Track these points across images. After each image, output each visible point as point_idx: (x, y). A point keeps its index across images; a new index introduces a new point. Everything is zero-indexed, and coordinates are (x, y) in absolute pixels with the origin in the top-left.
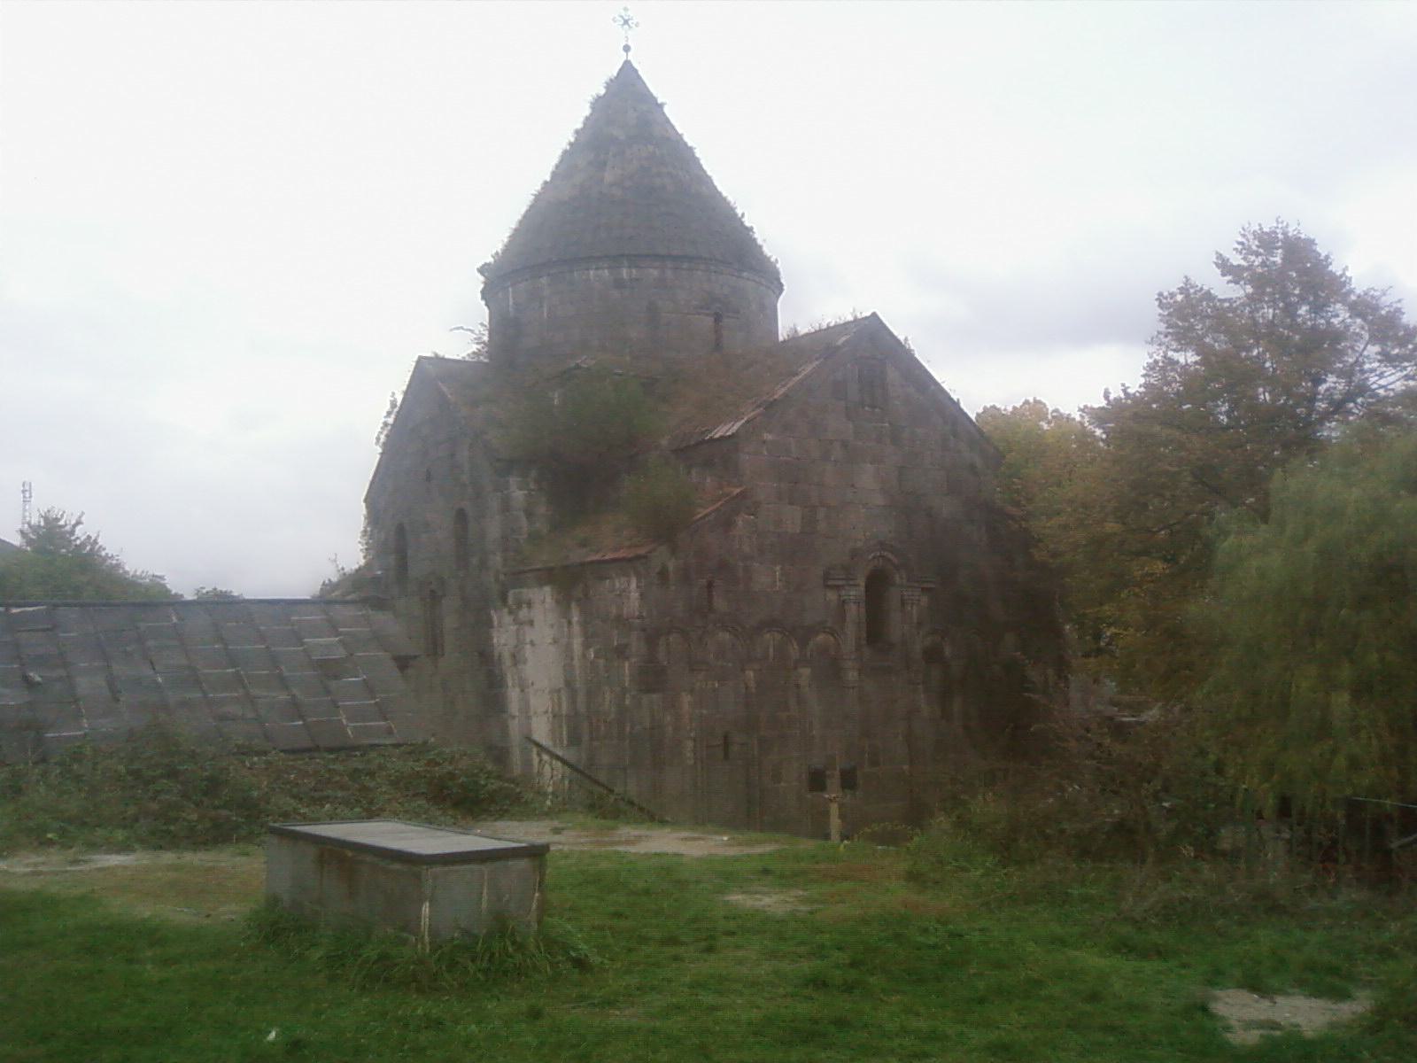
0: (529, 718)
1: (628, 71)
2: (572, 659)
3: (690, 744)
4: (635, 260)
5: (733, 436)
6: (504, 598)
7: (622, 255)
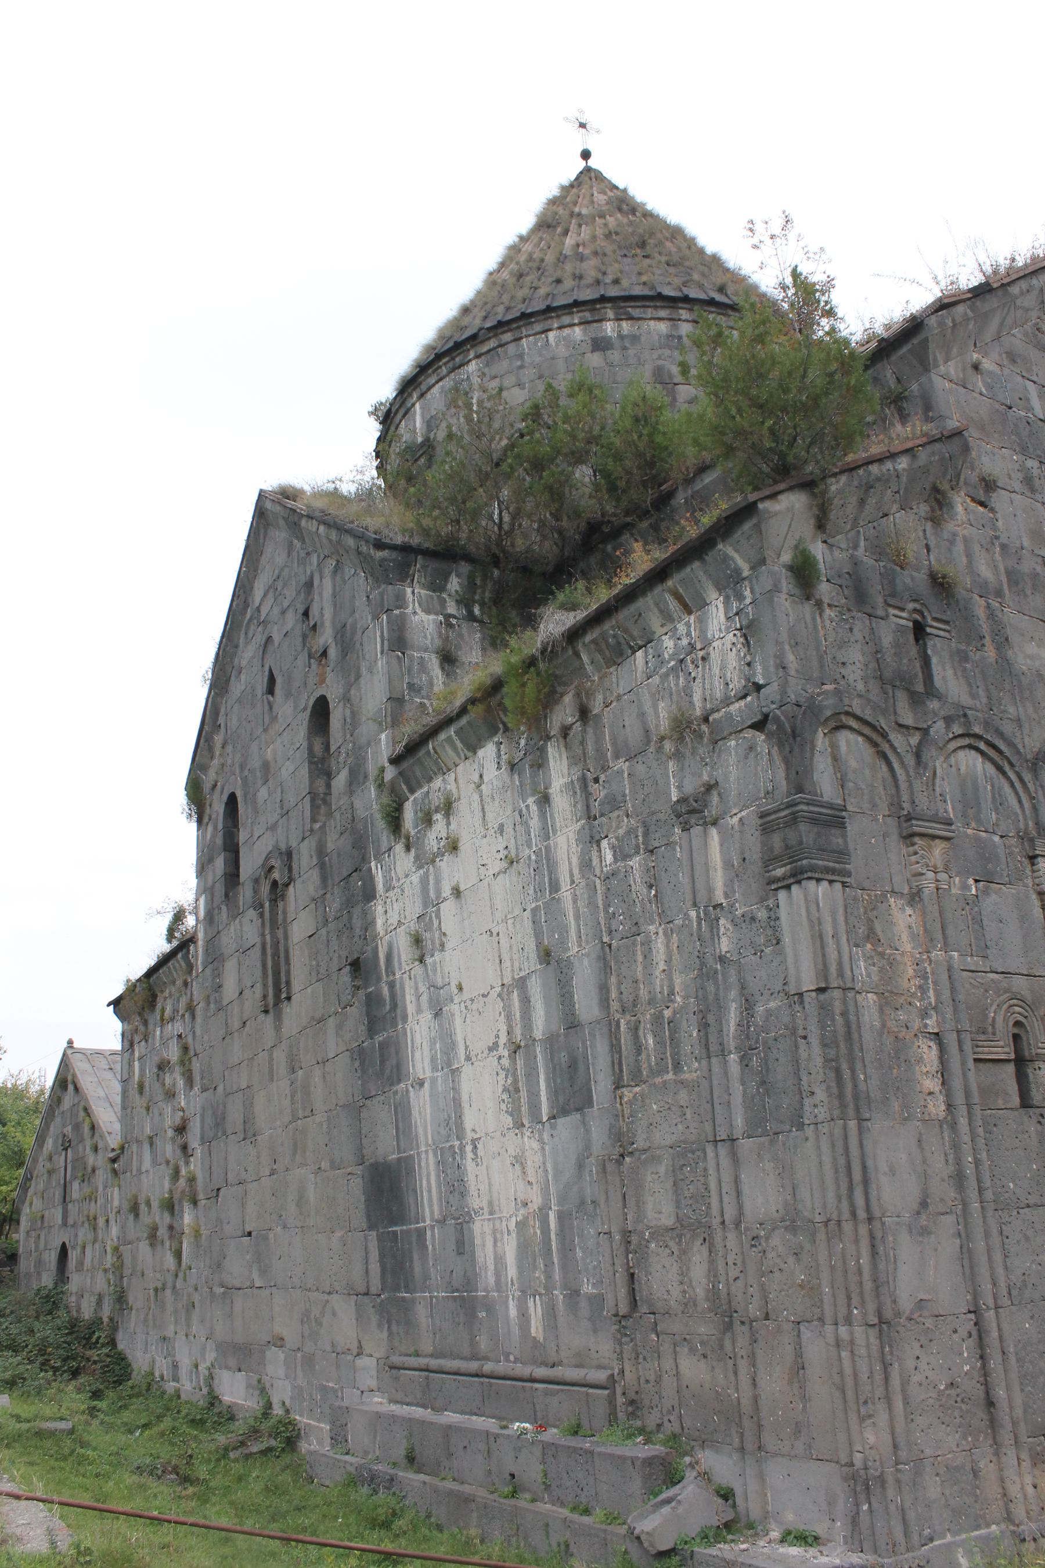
0: (455, 1072)
2: (555, 887)
3: (929, 1053)
4: (624, 304)
6: (395, 822)
7: (603, 299)
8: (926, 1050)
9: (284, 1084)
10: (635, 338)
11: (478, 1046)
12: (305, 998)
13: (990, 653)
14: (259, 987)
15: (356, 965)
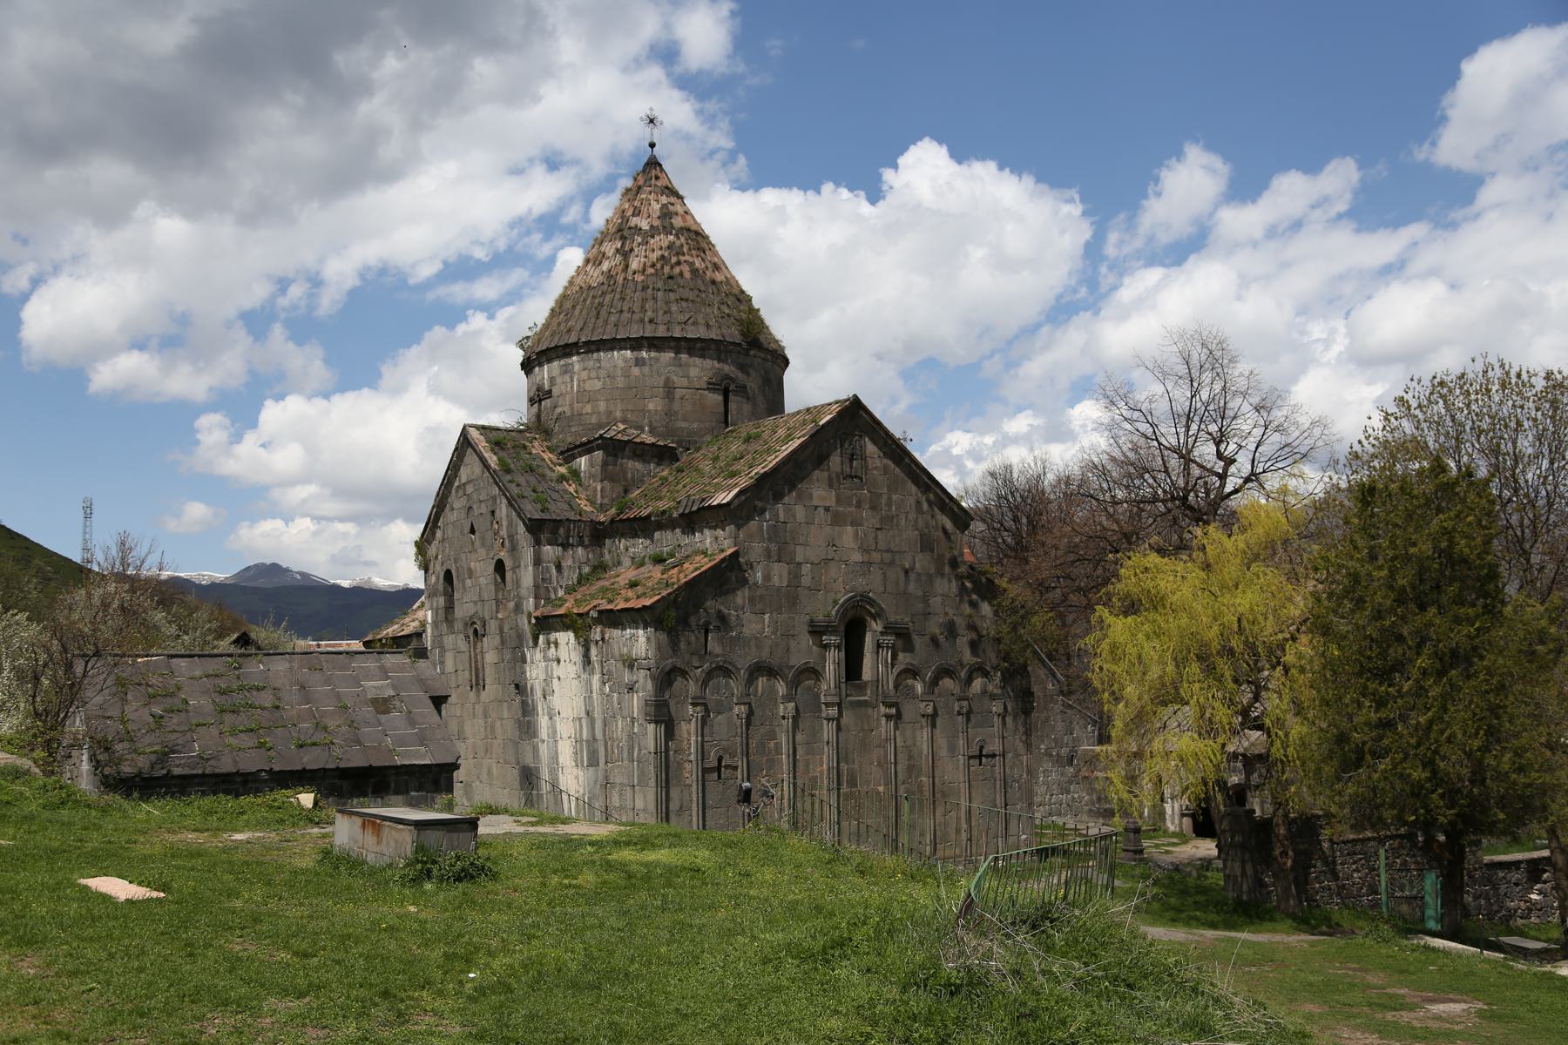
1: (653, 164)
4: (655, 343)
5: (728, 504)
6: (536, 639)
9: (481, 722)
10: (657, 359)
11: (565, 736)
12: (492, 690)
14: (467, 673)
15: (517, 686)
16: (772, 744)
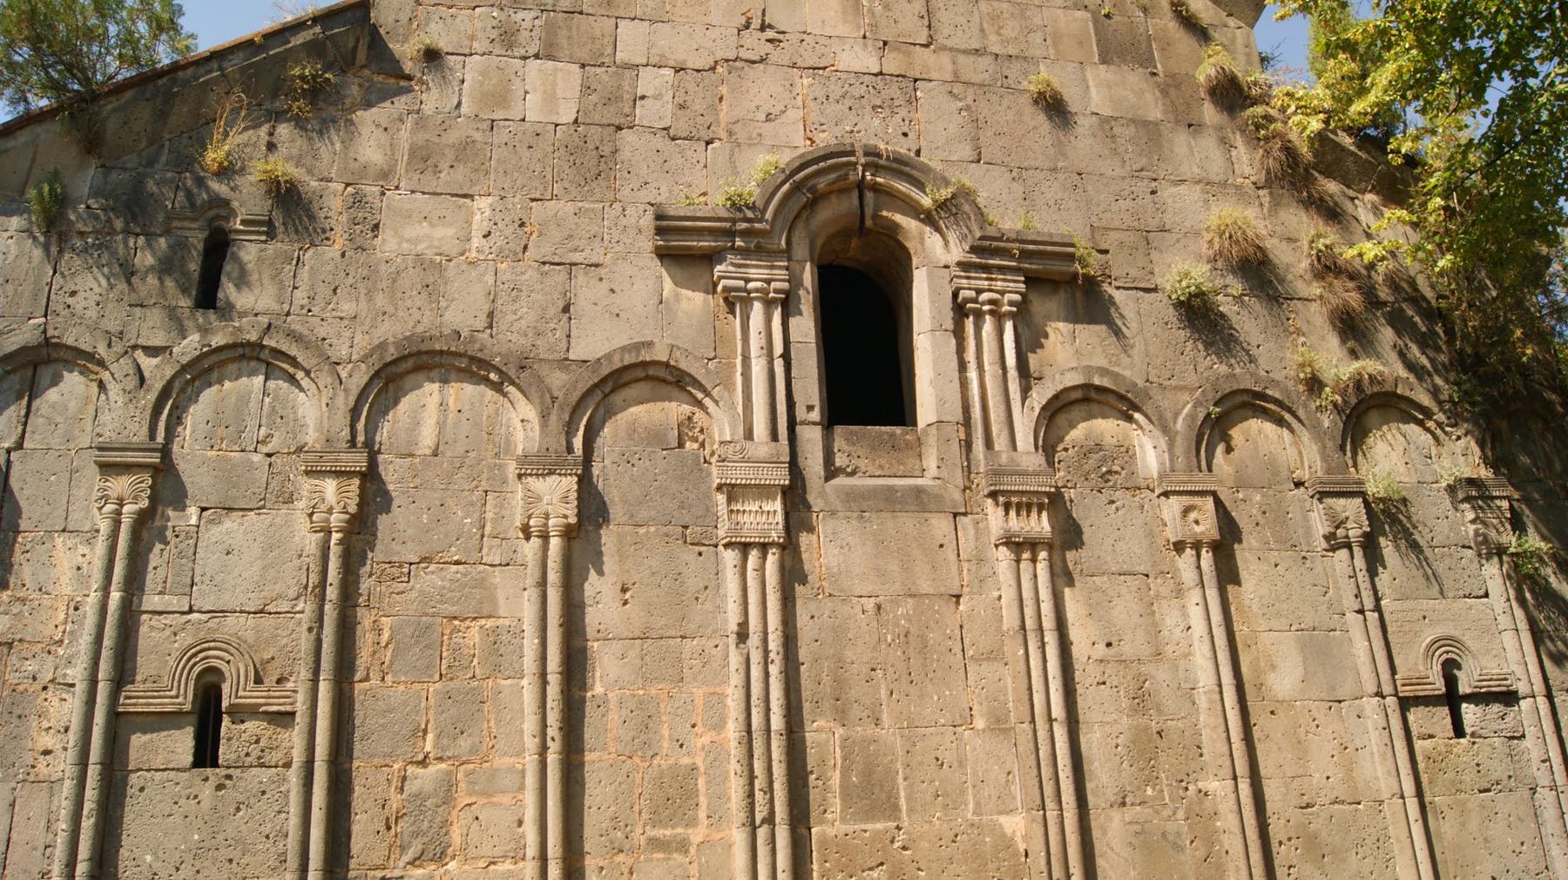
8: (56, 702)
13: (340, 241)
16: (473, 635)
